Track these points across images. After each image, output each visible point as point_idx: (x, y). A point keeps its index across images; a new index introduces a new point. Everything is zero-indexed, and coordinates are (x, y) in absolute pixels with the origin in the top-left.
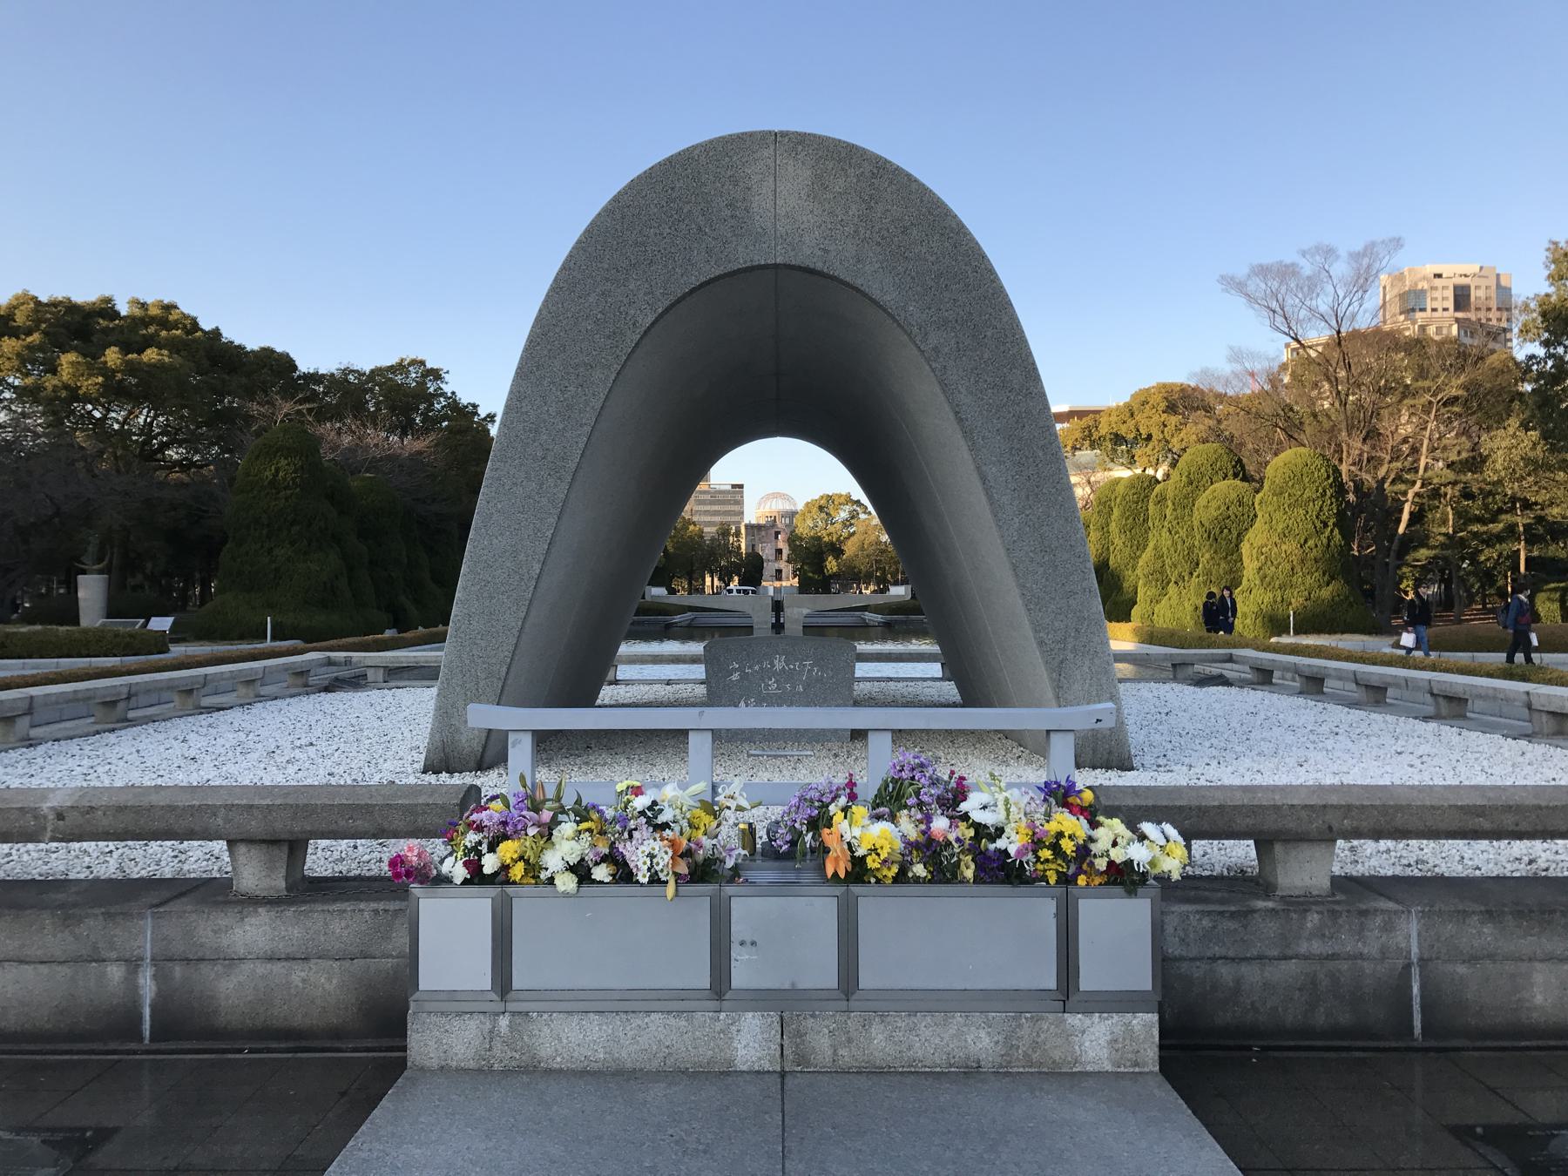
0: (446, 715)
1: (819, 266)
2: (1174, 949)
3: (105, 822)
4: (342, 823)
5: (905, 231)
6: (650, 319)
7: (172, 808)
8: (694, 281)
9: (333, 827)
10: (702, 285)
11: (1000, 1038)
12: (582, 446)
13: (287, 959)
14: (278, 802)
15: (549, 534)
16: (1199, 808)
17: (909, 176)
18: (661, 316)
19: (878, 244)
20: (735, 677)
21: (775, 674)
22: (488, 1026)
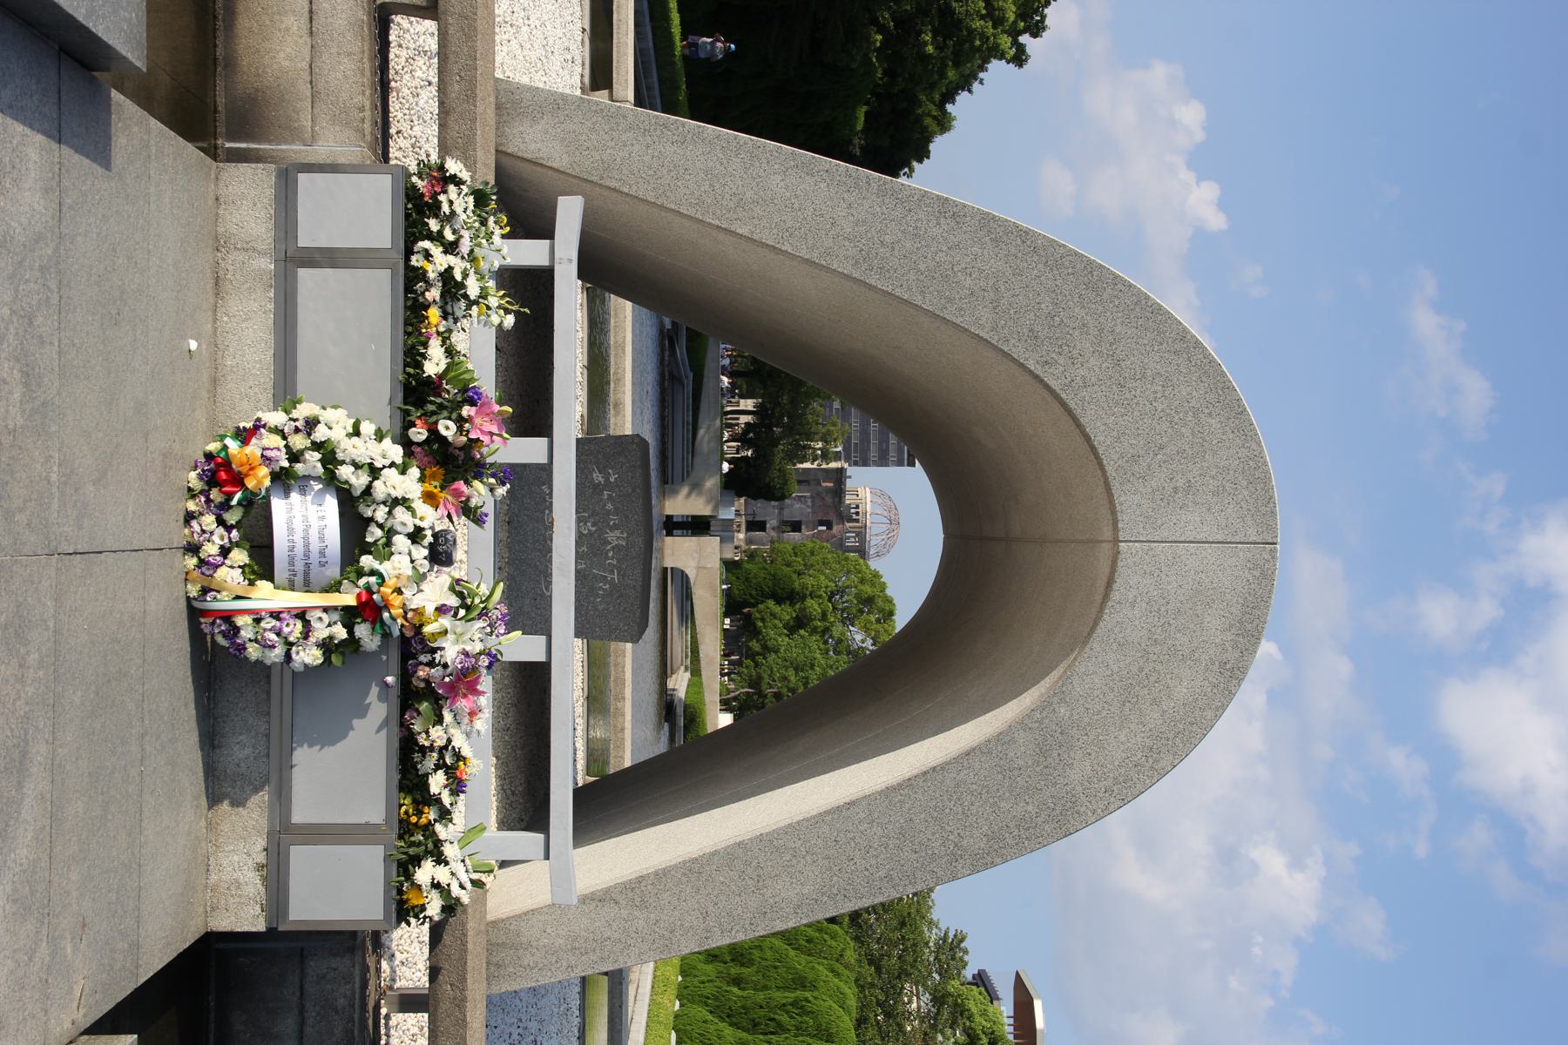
0: (554, 103)
1: (1115, 596)
2: (315, 967)
5: (1155, 702)
9: (452, 58)
10: (1093, 449)
11: (243, 769)
12: (898, 292)
13: (311, 12)
16: (464, 999)
17: (1224, 708)
20: (598, 477)
22: (261, 247)
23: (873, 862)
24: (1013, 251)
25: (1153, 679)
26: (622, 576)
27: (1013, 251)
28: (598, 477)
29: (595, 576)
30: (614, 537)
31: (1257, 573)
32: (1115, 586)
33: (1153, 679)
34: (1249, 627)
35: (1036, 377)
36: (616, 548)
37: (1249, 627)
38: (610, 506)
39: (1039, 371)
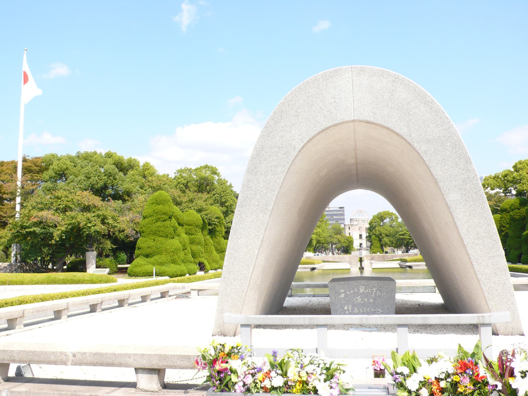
1: (372, 120)
3: (90, 359)
4: (179, 363)
6: (302, 145)
7: (114, 354)
8: (319, 129)
14: (153, 353)
15: (261, 237)
18: (306, 144)
19: (397, 109)
20: (343, 296)
21: (360, 294)
23: (471, 199)
24: (258, 162)
25: (400, 105)
26: (374, 287)
27: (258, 162)
28: (343, 296)
29: (375, 296)
30: (361, 291)
31: (362, 72)
32: (369, 120)
33: (400, 105)
34: (380, 74)
35: (299, 151)
36: (365, 289)
37: (380, 74)
38: (352, 292)
39: (297, 151)
